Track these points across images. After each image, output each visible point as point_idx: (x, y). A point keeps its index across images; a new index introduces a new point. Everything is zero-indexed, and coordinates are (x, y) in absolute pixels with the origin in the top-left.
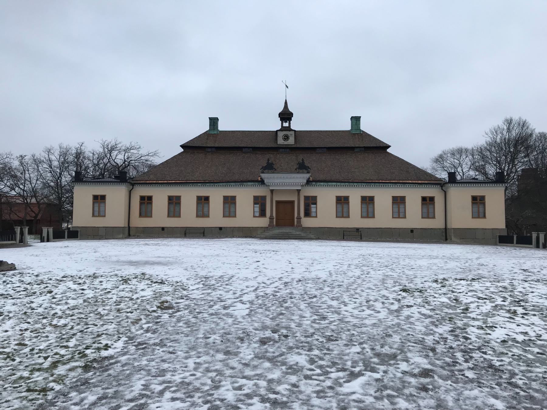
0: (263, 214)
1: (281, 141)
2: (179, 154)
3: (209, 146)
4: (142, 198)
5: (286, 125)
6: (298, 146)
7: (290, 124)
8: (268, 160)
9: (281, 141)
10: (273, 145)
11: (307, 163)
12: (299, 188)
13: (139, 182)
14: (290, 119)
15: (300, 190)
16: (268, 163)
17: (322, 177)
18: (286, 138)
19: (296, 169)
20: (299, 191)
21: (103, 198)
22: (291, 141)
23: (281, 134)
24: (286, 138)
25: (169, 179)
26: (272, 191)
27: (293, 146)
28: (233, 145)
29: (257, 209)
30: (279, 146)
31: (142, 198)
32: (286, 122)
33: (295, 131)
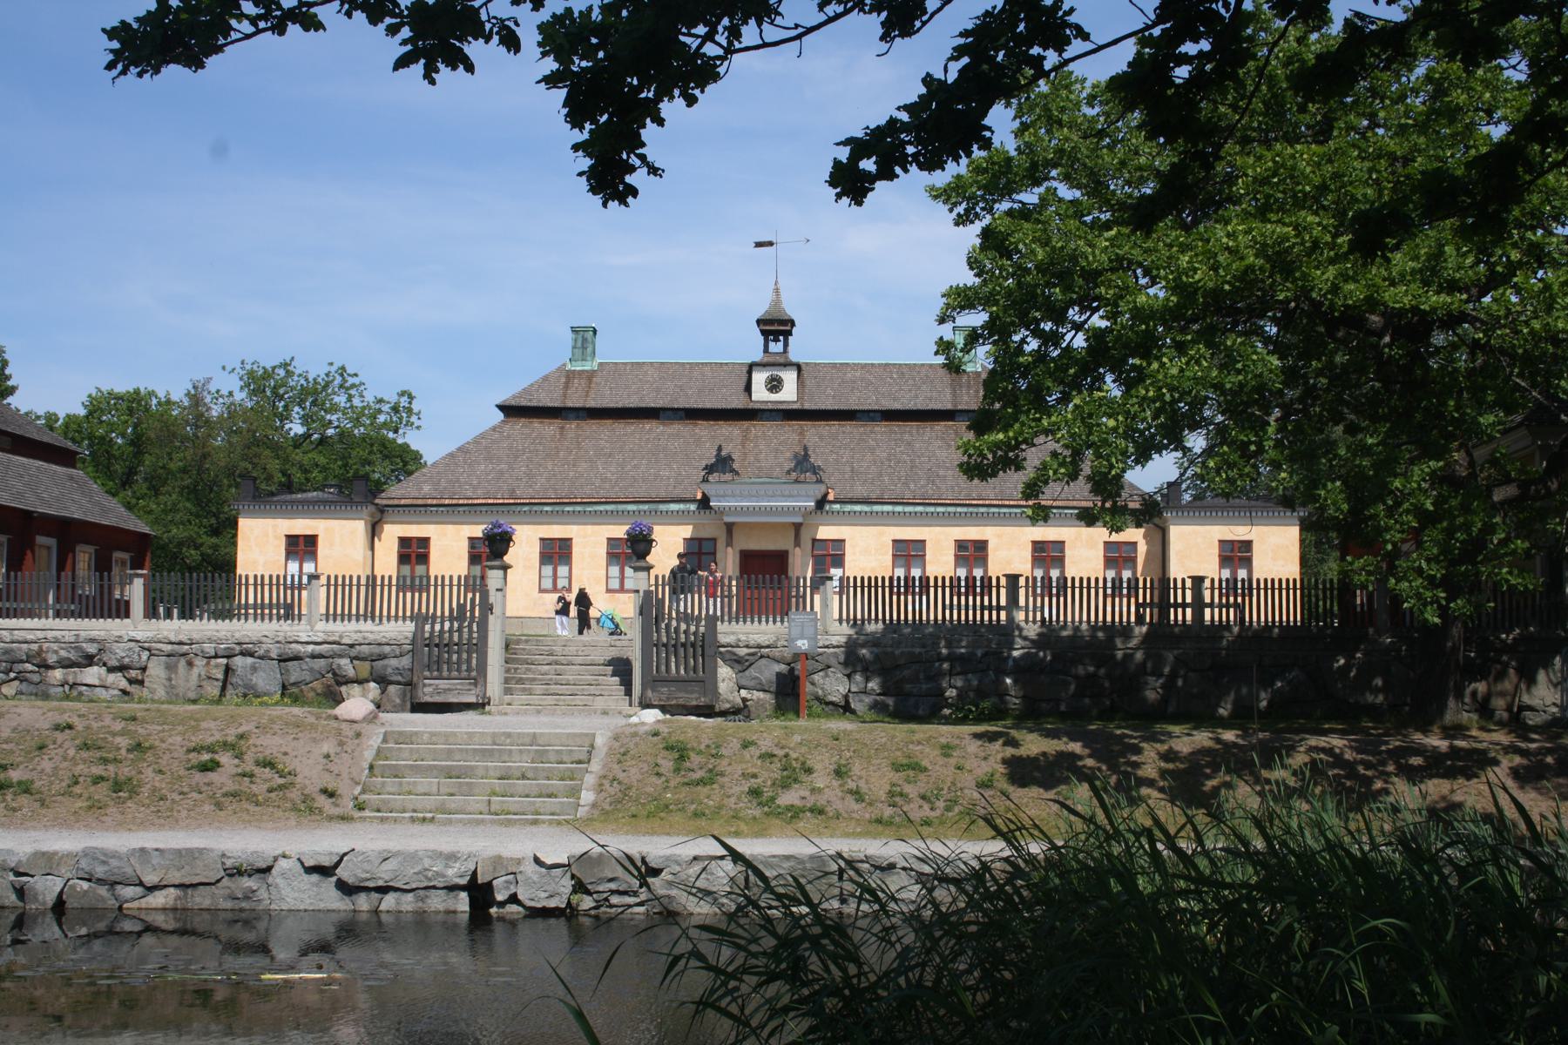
1: (760, 393)
2: (494, 429)
3: (570, 404)
4: (404, 542)
5: (776, 347)
6: (807, 406)
7: (786, 345)
8: (720, 449)
9: (760, 393)
10: (737, 402)
11: (815, 459)
12: (798, 520)
13: (396, 502)
14: (788, 334)
15: (800, 525)
16: (718, 455)
17: (860, 491)
18: (775, 385)
19: (788, 472)
20: (798, 527)
21: (311, 541)
22: (789, 393)
23: (760, 378)
24: (775, 385)
25: (469, 494)
26: (730, 527)
27: (795, 407)
28: (633, 402)
30: (757, 406)
31: (404, 542)
32: (776, 340)
33: (799, 367)
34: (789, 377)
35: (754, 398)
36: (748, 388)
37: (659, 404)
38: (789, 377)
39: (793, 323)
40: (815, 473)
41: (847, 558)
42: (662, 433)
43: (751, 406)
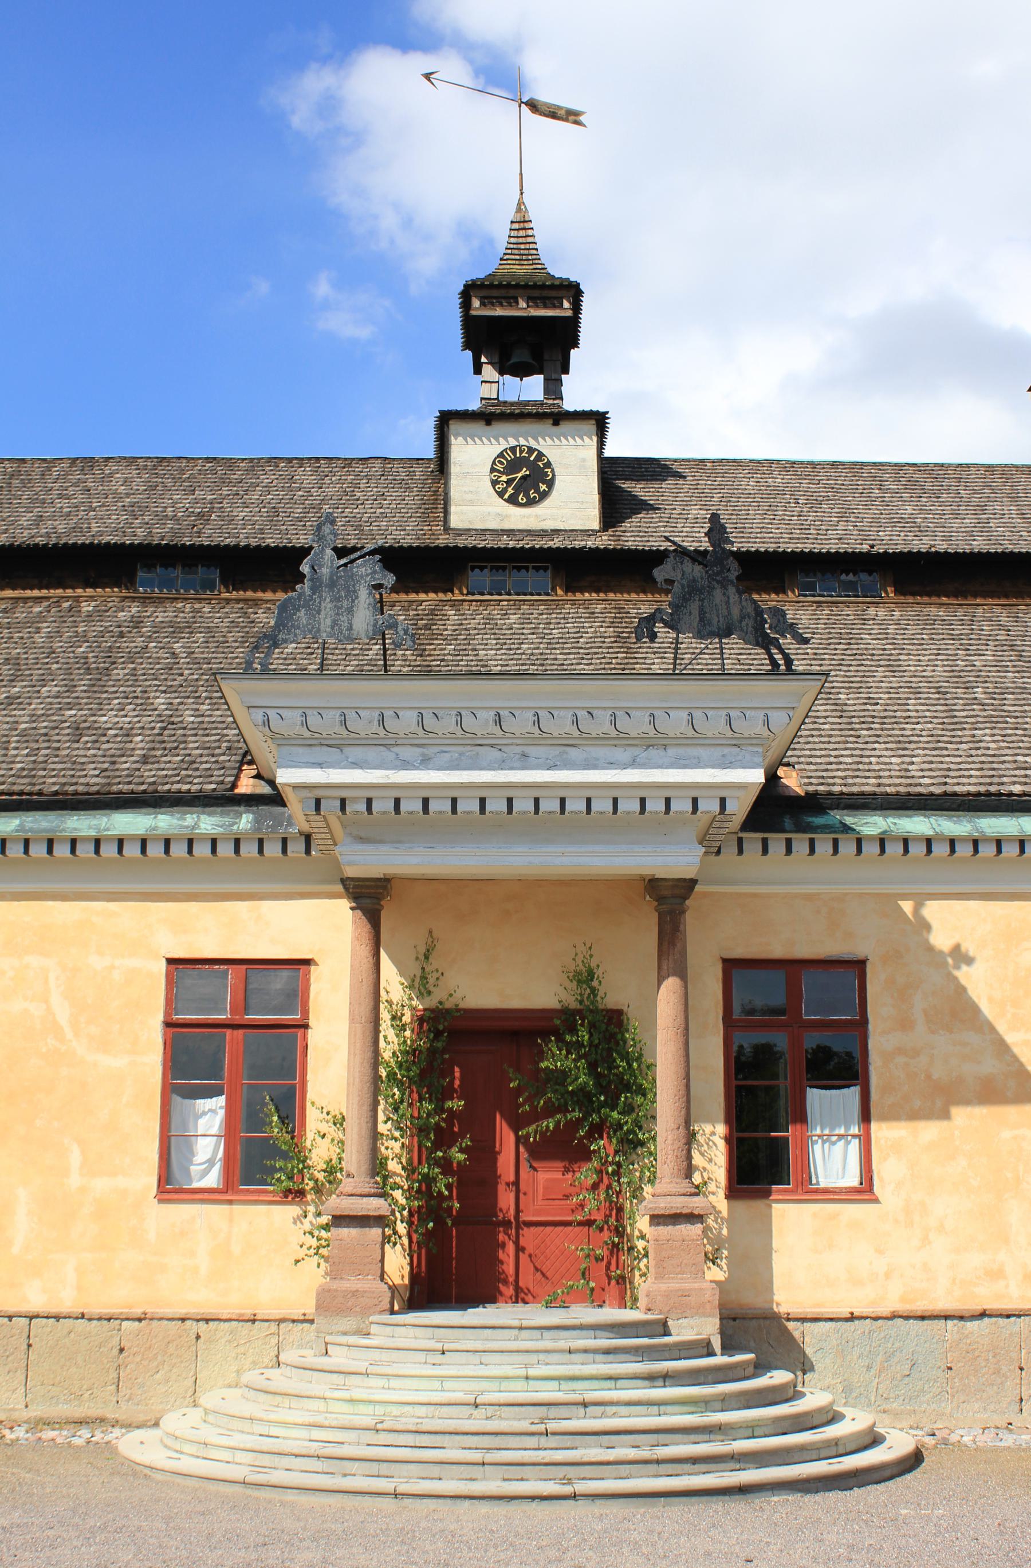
0: (265, 1162)
7: (553, 388)
9: (477, 506)
12: (677, 859)
18: (527, 478)
20: (669, 900)
22: (572, 509)
23: (474, 456)
24: (527, 478)
29: (210, 1116)
34: (573, 462)
35: (455, 522)
36: (439, 501)
37: (138, 535)
38: (573, 462)
39: (573, 291)
40: (765, 642)
41: (881, 1041)
42: (137, 623)
43: (442, 541)
